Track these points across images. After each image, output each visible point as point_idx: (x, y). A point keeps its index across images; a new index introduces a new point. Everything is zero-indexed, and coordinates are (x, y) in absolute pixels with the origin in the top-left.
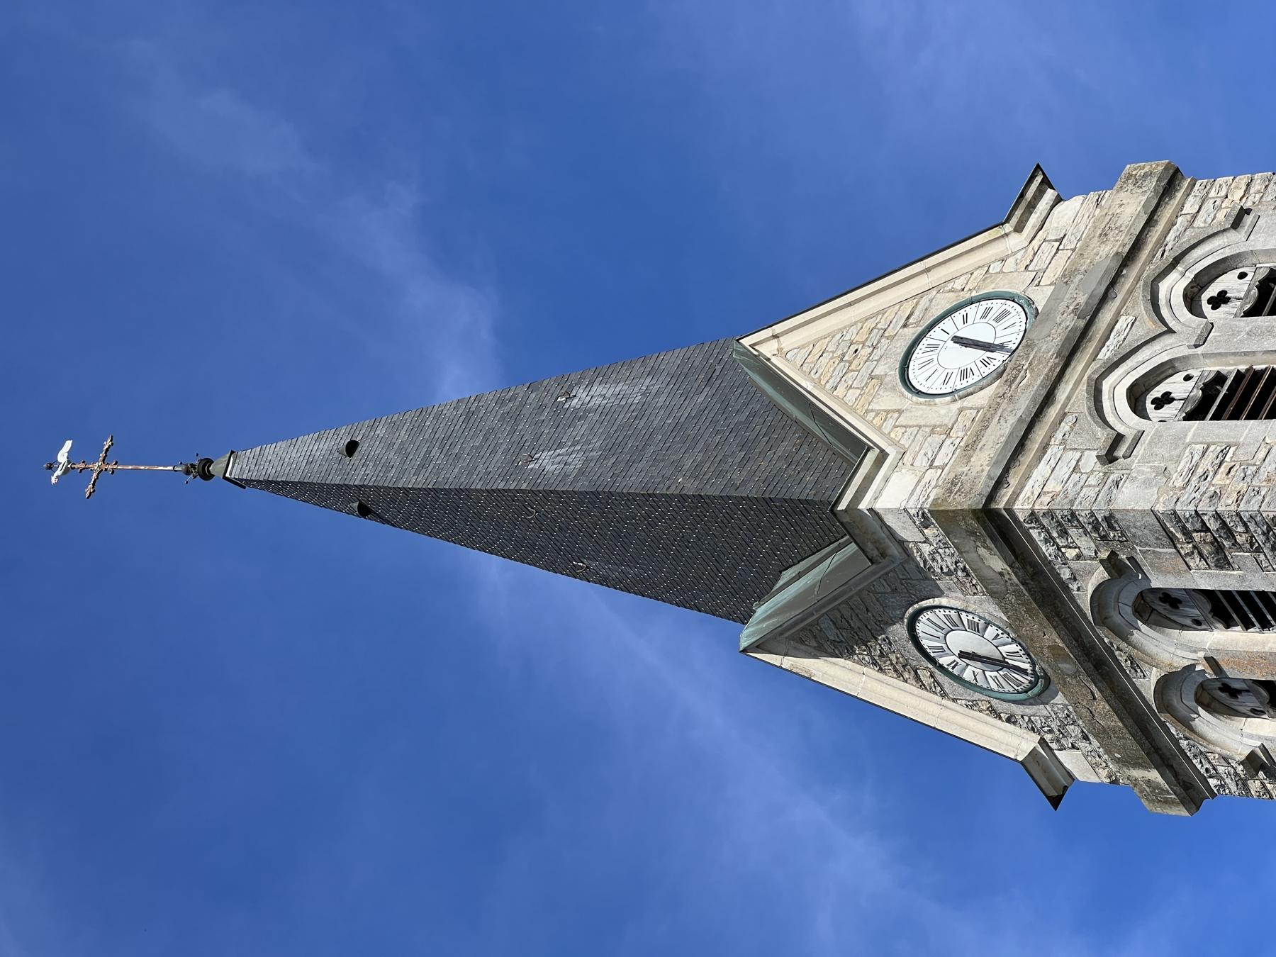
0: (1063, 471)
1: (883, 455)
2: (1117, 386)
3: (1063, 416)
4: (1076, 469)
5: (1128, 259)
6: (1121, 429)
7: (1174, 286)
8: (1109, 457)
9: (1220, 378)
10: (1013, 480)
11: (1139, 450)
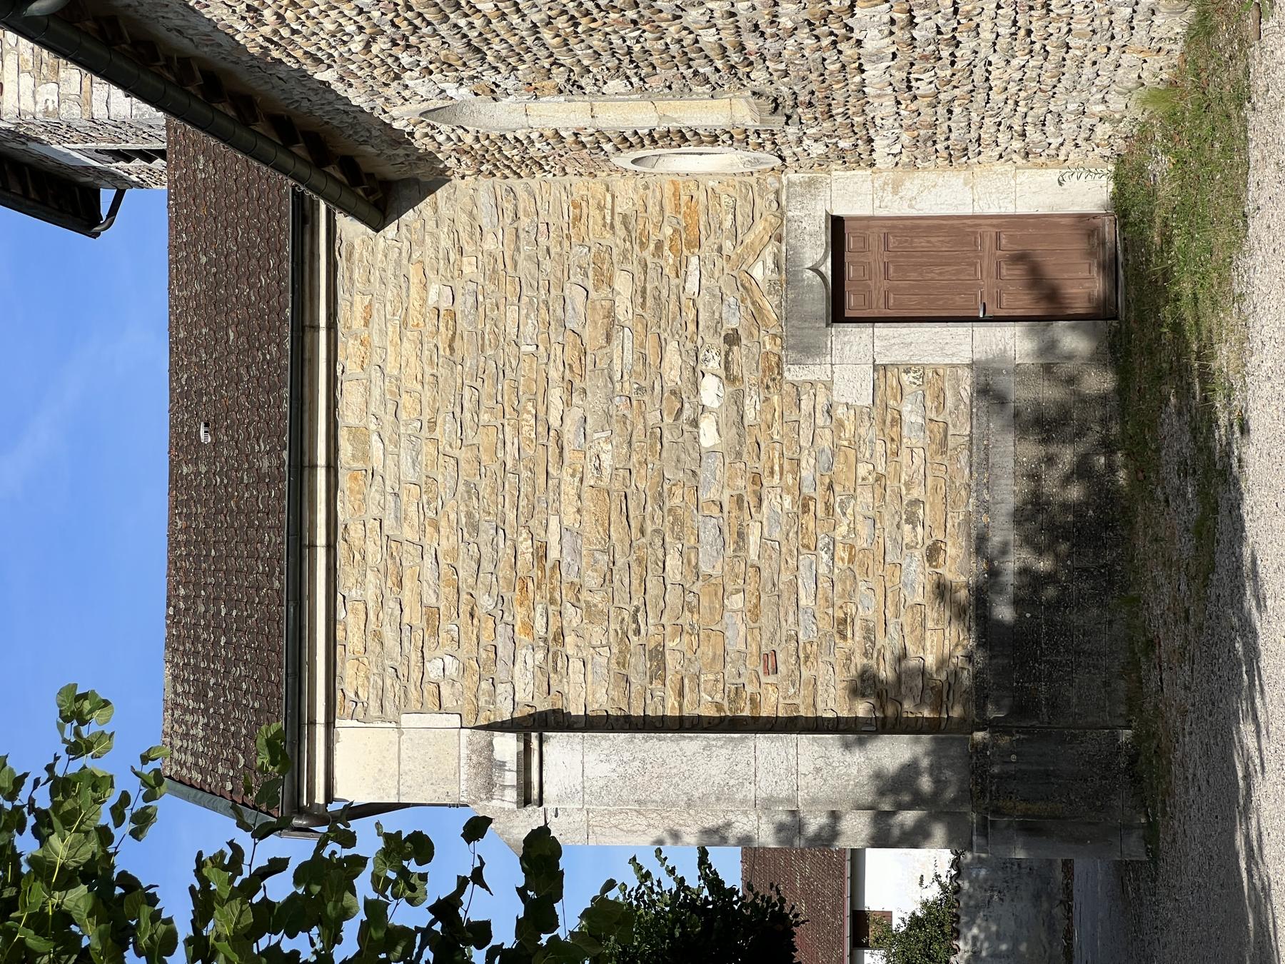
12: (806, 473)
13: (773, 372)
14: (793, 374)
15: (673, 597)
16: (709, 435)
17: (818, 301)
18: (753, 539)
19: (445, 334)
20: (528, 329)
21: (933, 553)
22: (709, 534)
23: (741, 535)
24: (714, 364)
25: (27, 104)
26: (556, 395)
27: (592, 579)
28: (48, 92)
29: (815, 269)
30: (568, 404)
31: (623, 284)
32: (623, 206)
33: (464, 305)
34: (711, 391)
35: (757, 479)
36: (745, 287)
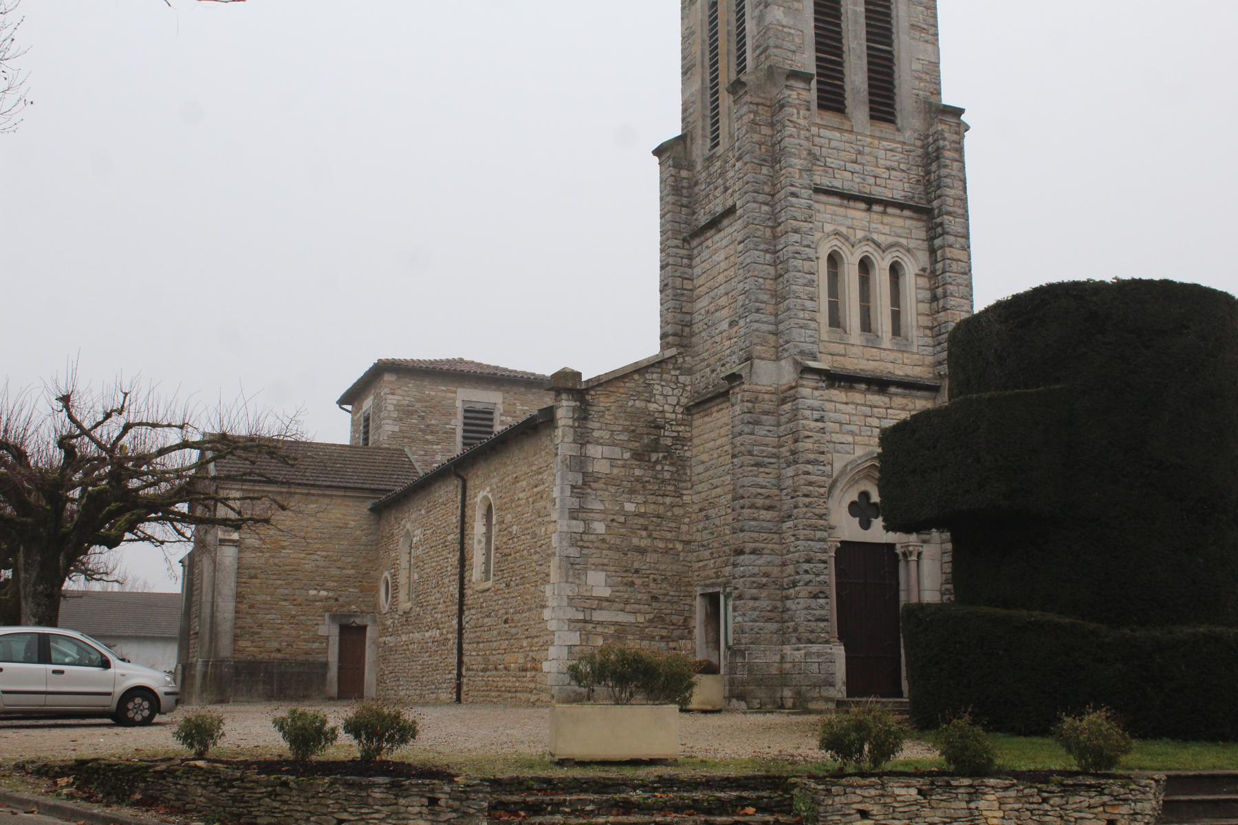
12: (301, 618)
13: (327, 610)
14: (327, 615)
15: (271, 582)
16: (312, 592)
17: (344, 621)
18: (284, 603)
19: (341, 525)
20: (342, 547)
21: (279, 650)
22: (287, 592)
23: (286, 600)
24: (330, 594)
25: (389, 401)
26: (324, 553)
27: (277, 561)
28: (391, 408)
29: (354, 622)
30: (322, 556)
31: (352, 572)
32: (372, 573)
33: (348, 531)
34: (324, 593)
35: (300, 605)
36: (349, 604)
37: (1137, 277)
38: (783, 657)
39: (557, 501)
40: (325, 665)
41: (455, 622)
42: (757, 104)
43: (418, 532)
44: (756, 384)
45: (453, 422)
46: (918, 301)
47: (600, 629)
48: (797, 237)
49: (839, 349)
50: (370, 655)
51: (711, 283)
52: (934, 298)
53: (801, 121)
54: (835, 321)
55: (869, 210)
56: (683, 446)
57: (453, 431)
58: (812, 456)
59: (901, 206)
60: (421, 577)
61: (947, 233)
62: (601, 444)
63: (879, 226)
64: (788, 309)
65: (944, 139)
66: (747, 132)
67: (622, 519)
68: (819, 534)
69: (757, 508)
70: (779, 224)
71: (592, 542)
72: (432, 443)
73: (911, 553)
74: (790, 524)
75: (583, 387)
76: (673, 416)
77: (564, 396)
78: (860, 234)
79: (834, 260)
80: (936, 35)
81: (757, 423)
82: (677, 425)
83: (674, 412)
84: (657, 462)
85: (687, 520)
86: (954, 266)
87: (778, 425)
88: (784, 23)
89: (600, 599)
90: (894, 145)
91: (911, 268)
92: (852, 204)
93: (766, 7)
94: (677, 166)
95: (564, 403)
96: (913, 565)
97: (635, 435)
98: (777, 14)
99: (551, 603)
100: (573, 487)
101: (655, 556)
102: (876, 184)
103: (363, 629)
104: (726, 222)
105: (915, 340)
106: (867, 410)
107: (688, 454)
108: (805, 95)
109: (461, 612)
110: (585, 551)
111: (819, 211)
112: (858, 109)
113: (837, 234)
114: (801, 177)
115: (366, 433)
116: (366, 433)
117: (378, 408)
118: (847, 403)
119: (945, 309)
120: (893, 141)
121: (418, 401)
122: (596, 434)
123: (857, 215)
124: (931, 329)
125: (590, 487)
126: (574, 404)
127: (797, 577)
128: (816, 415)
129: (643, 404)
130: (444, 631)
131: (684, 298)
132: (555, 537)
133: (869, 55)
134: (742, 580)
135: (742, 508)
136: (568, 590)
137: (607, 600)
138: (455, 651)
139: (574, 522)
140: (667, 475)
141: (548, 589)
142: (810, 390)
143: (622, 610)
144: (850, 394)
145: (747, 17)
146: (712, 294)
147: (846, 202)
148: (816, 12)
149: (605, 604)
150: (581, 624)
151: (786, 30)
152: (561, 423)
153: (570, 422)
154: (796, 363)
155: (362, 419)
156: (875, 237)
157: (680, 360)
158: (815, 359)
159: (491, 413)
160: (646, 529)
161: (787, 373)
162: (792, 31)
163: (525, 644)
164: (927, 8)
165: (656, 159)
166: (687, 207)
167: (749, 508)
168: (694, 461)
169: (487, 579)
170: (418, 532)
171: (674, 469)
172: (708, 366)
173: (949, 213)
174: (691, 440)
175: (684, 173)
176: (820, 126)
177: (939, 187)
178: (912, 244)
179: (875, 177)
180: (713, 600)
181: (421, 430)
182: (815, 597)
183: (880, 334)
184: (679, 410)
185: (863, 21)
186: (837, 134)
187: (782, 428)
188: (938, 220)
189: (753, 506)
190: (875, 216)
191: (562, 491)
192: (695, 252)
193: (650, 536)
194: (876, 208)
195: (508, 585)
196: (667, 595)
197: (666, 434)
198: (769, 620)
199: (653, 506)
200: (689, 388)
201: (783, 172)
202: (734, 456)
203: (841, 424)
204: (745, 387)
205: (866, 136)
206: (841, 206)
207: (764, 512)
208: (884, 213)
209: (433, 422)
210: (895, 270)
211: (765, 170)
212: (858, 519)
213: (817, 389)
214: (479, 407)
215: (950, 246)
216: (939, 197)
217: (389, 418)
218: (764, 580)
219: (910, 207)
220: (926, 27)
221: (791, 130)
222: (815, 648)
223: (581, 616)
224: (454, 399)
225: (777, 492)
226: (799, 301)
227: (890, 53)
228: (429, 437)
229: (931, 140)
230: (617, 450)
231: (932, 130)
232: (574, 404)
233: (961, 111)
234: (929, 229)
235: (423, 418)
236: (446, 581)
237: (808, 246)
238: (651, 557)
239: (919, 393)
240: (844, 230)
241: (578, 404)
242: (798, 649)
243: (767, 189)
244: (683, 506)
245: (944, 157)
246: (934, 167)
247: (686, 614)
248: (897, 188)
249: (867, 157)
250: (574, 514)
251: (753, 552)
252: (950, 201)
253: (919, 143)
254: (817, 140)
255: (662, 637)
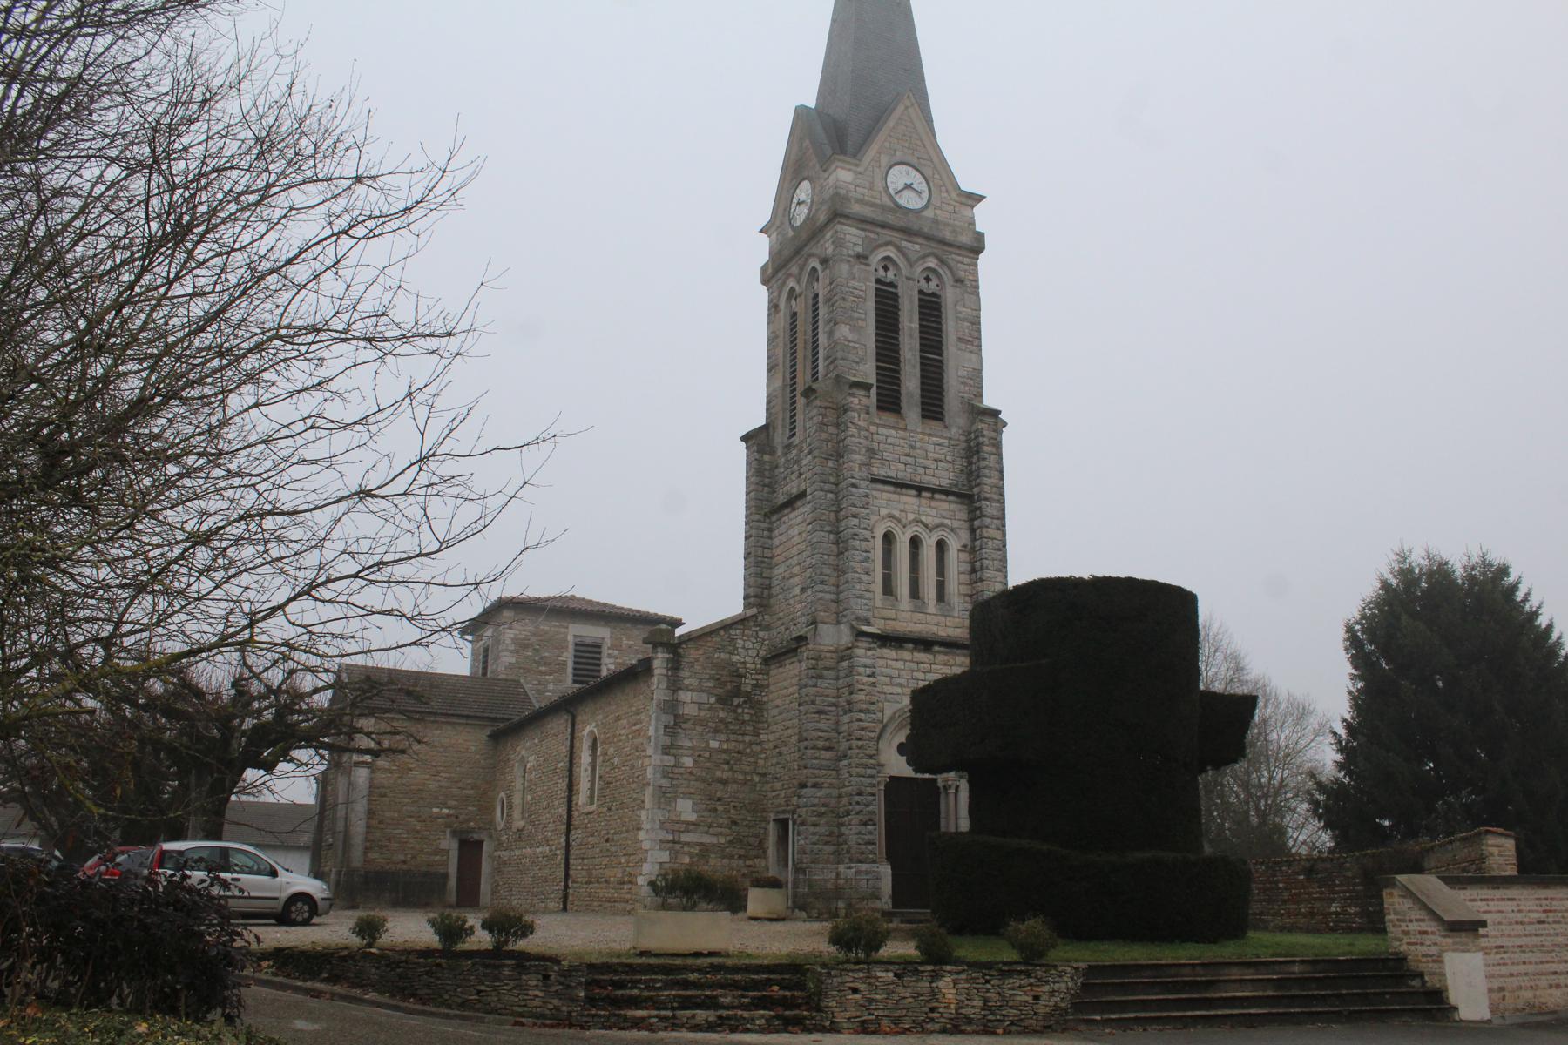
0: (854, 240)
1: (857, 165)
2: (890, 252)
3: (878, 234)
4: (855, 244)
5: (943, 242)
6: (871, 258)
7: (932, 263)
8: (859, 256)
9: (896, 287)
10: (849, 222)
11: (862, 267)
14: (448, 831)
15: (398, 800)
16: (435, 810)
21: (404, 862)
22: (413, 809)
23: (411, 817)
24: (452, 812)
25: (507, 635)
27: (404, 781)
28: (508, 641)
33: (468, 755)
34: (445, 811)
36: (468, 821)
37: (1107, 575)
38: (838, 874)
39: (652, 739)
40: (446, 876)
41: (563, 840)
42: (826, 408)
43: (531, 758)
44: (820, 644)
45: (564, 654)
46: (960, 573)
47: (686, 849)
48: (855, 521)
49: (891, 614)
50: (486, 867)
51: (787, 554)
52: (973, 571)
53: (862, 424)
54: (888, 589)
55: (919, 496)
56: (761, 692)
57: (564, 664)
58: (864, 706)
59: (947, 493)
60: (533, 799)
61: (985, 516)
62: (691, 690)
63: (928, 510)
64: (847, 582)
65: (983, 436)
66: (816, 431)
67: (707, 755)
68: (869, 772)
69: (818, 749)
70: (842, 510)
71: (681, 774)
72: (546, 674)
73: (950, 787)
74: (845, 762)
75: (676, 641)
76: (753, 666)
77: (660, 649)
78: (911, 517)
79: (888, 538)
80: (980, 346)
81: (820, 677)
82: (757, 674)
83: (754, 663)
84: (738, 706)
85: (763, 756)
86: (990, 544)
87: (837, 679)
88: (850, 338)
89: (688, 823)
90: (941, 441)
91: (954, 545)
92: (904, 491)
93: (835, 324)
94: (761, 451)
95: (660, 655)
96: (952, 797)
97: (720, 683)
98: (844, 331)
99: (646, 826)
100: (666, 727)
101: (735, 786)
102: (925, 474)
103: (480, 843)
104: (799, 503)
105: (956, 606)
106: (914, 666)
107: (765, 699)
108: (865, 401)
109: (568, 832)
110: (675, 782)
111: (876, 497)
112: (912, 413)
113: (891, 516)
114: (860, 469)
115: (485, 662)
116: (485, 662)
117: (497, 640)
118: (896, 660)
119: (981, 580)
120: (941, 437)
121: (534, 635)
122: (686, 682)
123: (909, 500)
124: (971, 596)
125: (680, 727)
126: (667, 656)
127: (850, 808)
128: (869, 671)
129: (727, 655)
130: (554, 847)
131: (763, 565)
132: (650, 770)
133: (921, 364)
134: (804, 809)
135: (806, 748)
136: (660, 816)
137: (693, 824)
138: (563, 866)
139: (666, 757)
140: (747, 717)
141: (643, 815)
142: (863, 651)
143: (706, 833)
144: (899, 652)
145: (820, 330)
146: (788, 563)
147: (899, 490)
148: (877, 328)
149: (692, 827)
150: (670, 845)
151: (851, 344)
152: (657, 672)
153: (664, 672)
154: (852, 627)
155: (482, 649)
156: (923, 518)
157: (760, 618)
158: (869, 623)
159: (600, 647)
160: (728, 763)
161: (846, 638)
162: (857, 346)
163: (623, 861)
164: (973, 324)
165: (743, 445)
166: (768, 486)
167: (812, 748)
168: (770, 704)
169: (592, 803)
170: (531, 758)
171: (753, 712)
172: (783, 624)
173: (986, 499)
174: (768, 686)
175: (767, 458)
176: (878, 425)
177: (978, 477)
178: (956, 524)
179: (925, 468)
180: (783, 824)
181: (535, 662)
182: (865, 824)
183: (926, 600)
184: (758, 661)
185: (917, 335)
186: (893, 432)
187: (841, 681)
188: (977, 505)
189: (815, 747)
190: (924, 501)
191: (656, 730)
192: (775, 525)
193: (731, 769)
194: (925, 494)
195: (609, 809)
196: (745, 819)
197: (747, 681)
198: (826, 843)
199: (734, 744)
200: (766, 642)
201: (846, 466)
202: (800, 705)
203: (891, 677)
204: (810, 647)
205: (918, 433)
206: (894, 493)
207: (823, 752)
208: (932, 498)
209: (547, 654)
210: (941, 546)
211: (830, 464)
212: (905, 758)
213: (870, 649)
214: (588, 641)
215: (987, 527)
216: (979, 485)
217: (507, 650)
218: (823, 809)
219: (954, 494)
220: (970, 339)
221: (853, 431)
222: (864, 867)
223: (671, 838)
224: (566, 634)
225: (836, 735)
226: (856, 575)
227: (941, 361)
228: (543, 668)
229: (972, 436)
230: (705, 696)
231: (974, 428)
232: (667, 656)
233: (999, 412)
234: (971, 512)
235: (537, 650)
236: (556, 803)
237: (865, 529)
238: (732, 787)
239: (959, 651)
240: (896, 513)
241: (671, 656)
242: (850, 868)
243: (832, 479)
244: (760, 743)
245: (983, 452)
246: (975, 459)
247: (761, 836)
248: (944, 476)
249: (918, 451)
250: (666, 750)
251: (815, 786)
252: (987, 488)
253: (963, 438)
254: (875, 437)
255: (740, 856)
